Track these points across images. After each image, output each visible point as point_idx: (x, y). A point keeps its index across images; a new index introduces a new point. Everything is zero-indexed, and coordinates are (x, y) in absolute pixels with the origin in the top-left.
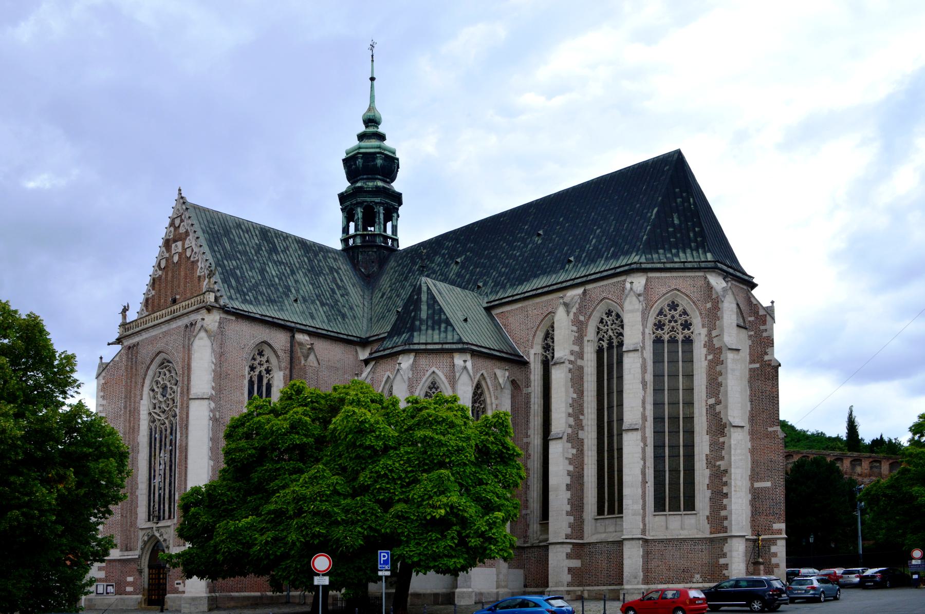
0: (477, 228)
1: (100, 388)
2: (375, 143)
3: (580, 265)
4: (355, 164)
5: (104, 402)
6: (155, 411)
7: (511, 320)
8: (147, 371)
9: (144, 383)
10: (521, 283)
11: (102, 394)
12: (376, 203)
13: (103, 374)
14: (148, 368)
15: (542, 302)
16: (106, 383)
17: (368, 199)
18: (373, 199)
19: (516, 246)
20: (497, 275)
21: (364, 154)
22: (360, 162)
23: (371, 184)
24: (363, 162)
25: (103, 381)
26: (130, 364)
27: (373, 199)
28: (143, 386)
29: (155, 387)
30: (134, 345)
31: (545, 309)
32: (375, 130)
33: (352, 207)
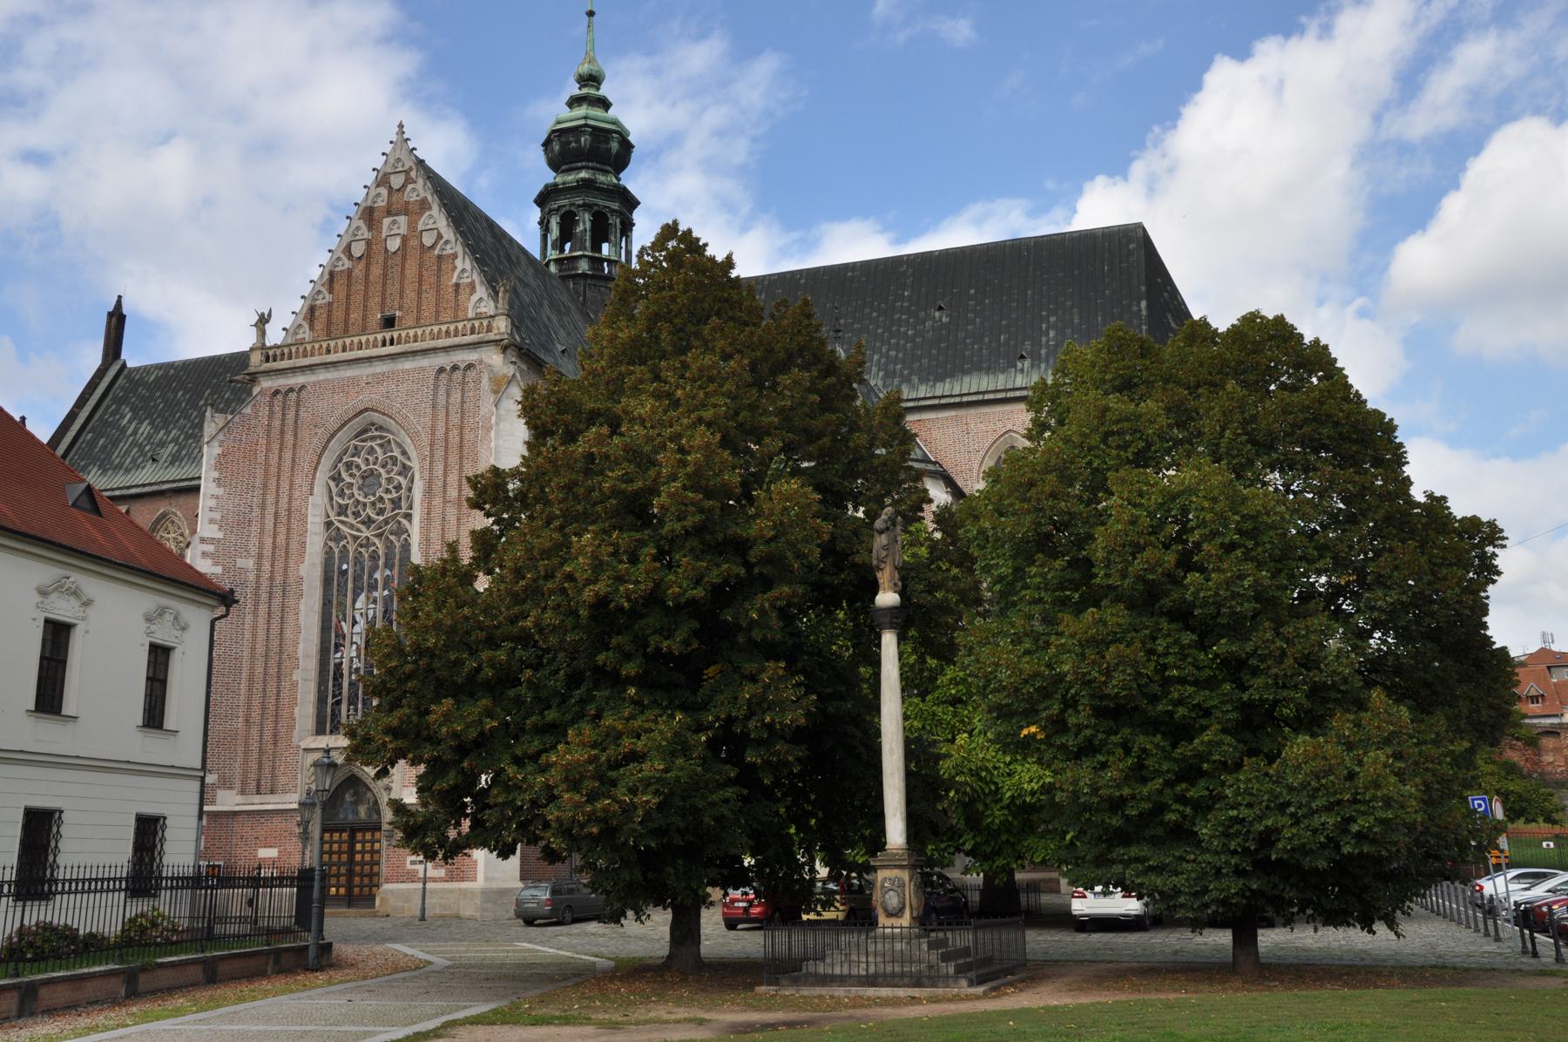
0: (803, 281)
1: (213, 462)
2: (597, 112)
3: (1043, 366)
4: (578, 141)
5: (220, 491)
6: (343, 518)
7: (936, 434)
8: (329, 441)
9: (318, 463)
10: (941, 378)
11: (216, 474)
12: (613, 211)
13: (221, 437)
14: (333, 436)
15: (994, 413)
16: (224, 455)
17: (601, 202)
18: (608, 204)
19: (900, 319)
20: (883, 360)
21: (595, 128)
22: (584, 140)
23: (601, 178)
24: (593, 141)
25: (219, 451)
26: (277, 423)
27: (608, 204)
28: (316, 468)
29: (344, 475)
30: (291, 390)
31: (1000, 425)
32: (592, 91)
33: (573, 209)
